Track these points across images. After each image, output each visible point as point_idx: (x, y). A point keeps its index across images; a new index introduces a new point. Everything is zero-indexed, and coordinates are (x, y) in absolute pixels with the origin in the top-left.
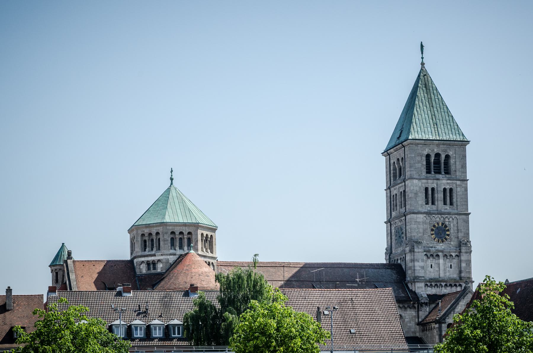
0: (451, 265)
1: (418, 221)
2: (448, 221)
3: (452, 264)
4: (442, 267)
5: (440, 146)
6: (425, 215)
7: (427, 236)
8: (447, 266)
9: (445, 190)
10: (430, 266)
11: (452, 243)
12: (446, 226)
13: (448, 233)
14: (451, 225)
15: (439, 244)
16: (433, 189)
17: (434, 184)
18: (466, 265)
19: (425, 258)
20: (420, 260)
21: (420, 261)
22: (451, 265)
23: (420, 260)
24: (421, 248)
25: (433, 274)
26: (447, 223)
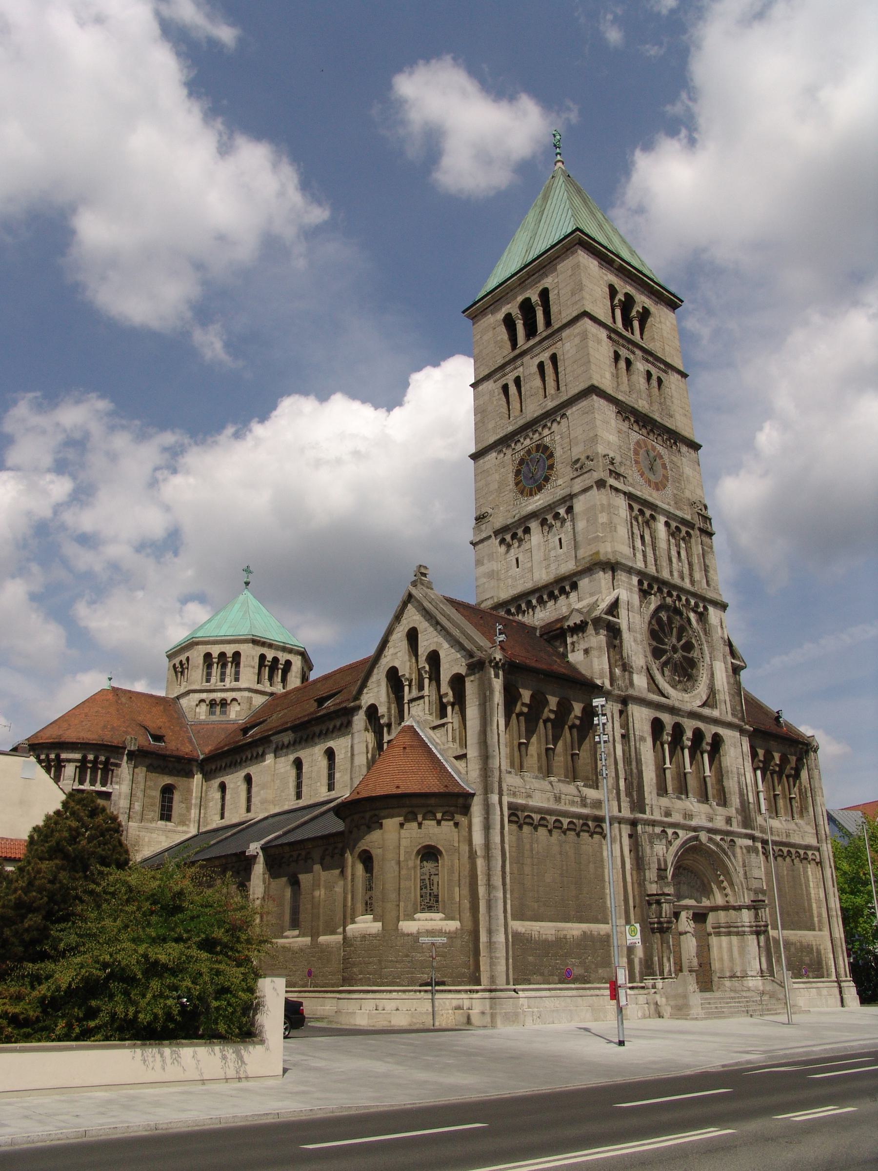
0: (560, 540)
1: (486, 468)
2: (550, 432)
3: (562, 536)
4: (538, 556)
5: (527, 282)
6: (499, 447)
7: (506, 493)
8: (551, 545)
9: (541, 366)
10: (514, 561)
11: (560, 482)
12: (546, 448)
13: (550, 462)
14: (556, 438)
15: (531, 501)
16: (518, 381)
17: (518, 369)
18: (588, 521)
19: (503, 548)
20: (486, 558)
21: (485, 561)
22: (560, 540)
23: (486, 558)
24: (486, 528)
25: (521, 581)
26: (547, 440)
